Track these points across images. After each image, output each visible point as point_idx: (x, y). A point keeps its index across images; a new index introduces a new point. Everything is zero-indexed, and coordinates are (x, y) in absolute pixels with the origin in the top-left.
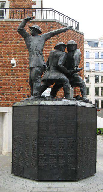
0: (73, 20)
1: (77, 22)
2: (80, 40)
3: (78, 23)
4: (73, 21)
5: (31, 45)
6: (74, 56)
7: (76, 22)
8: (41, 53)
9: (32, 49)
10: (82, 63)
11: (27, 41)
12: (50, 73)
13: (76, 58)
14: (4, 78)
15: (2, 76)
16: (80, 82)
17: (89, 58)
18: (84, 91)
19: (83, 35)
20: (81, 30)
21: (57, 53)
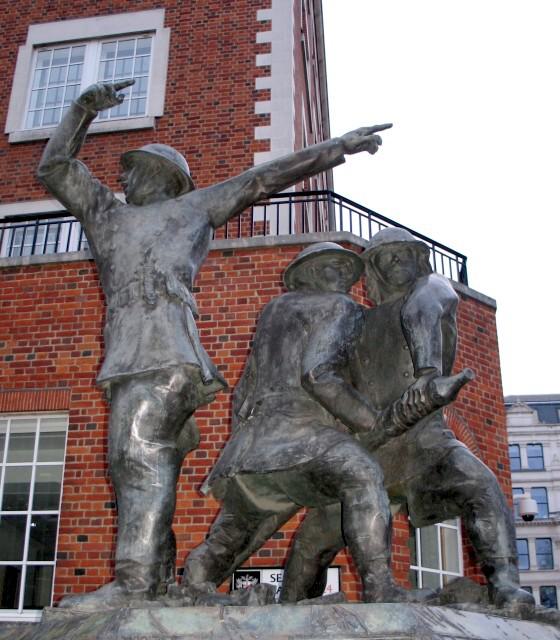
0: (435, 243)
1: (458, 255)
2: (480, 330)
3: (465, 258)
4: (436, 248)
5: (114, 251)
6: (411, 310)
7: (454, 257)
8: (174, 285)
9: (122, 274)
10: (498, 439)
11: (94, 232)
12: (256, 436)
13: (420, 314)
14: (98, 522)
15: (89, 514)
16: (462, 476)
17: (543, 470)
18: (495, 541)
19: (493, 309)
20: (477, 283)
21: (297, 307)
